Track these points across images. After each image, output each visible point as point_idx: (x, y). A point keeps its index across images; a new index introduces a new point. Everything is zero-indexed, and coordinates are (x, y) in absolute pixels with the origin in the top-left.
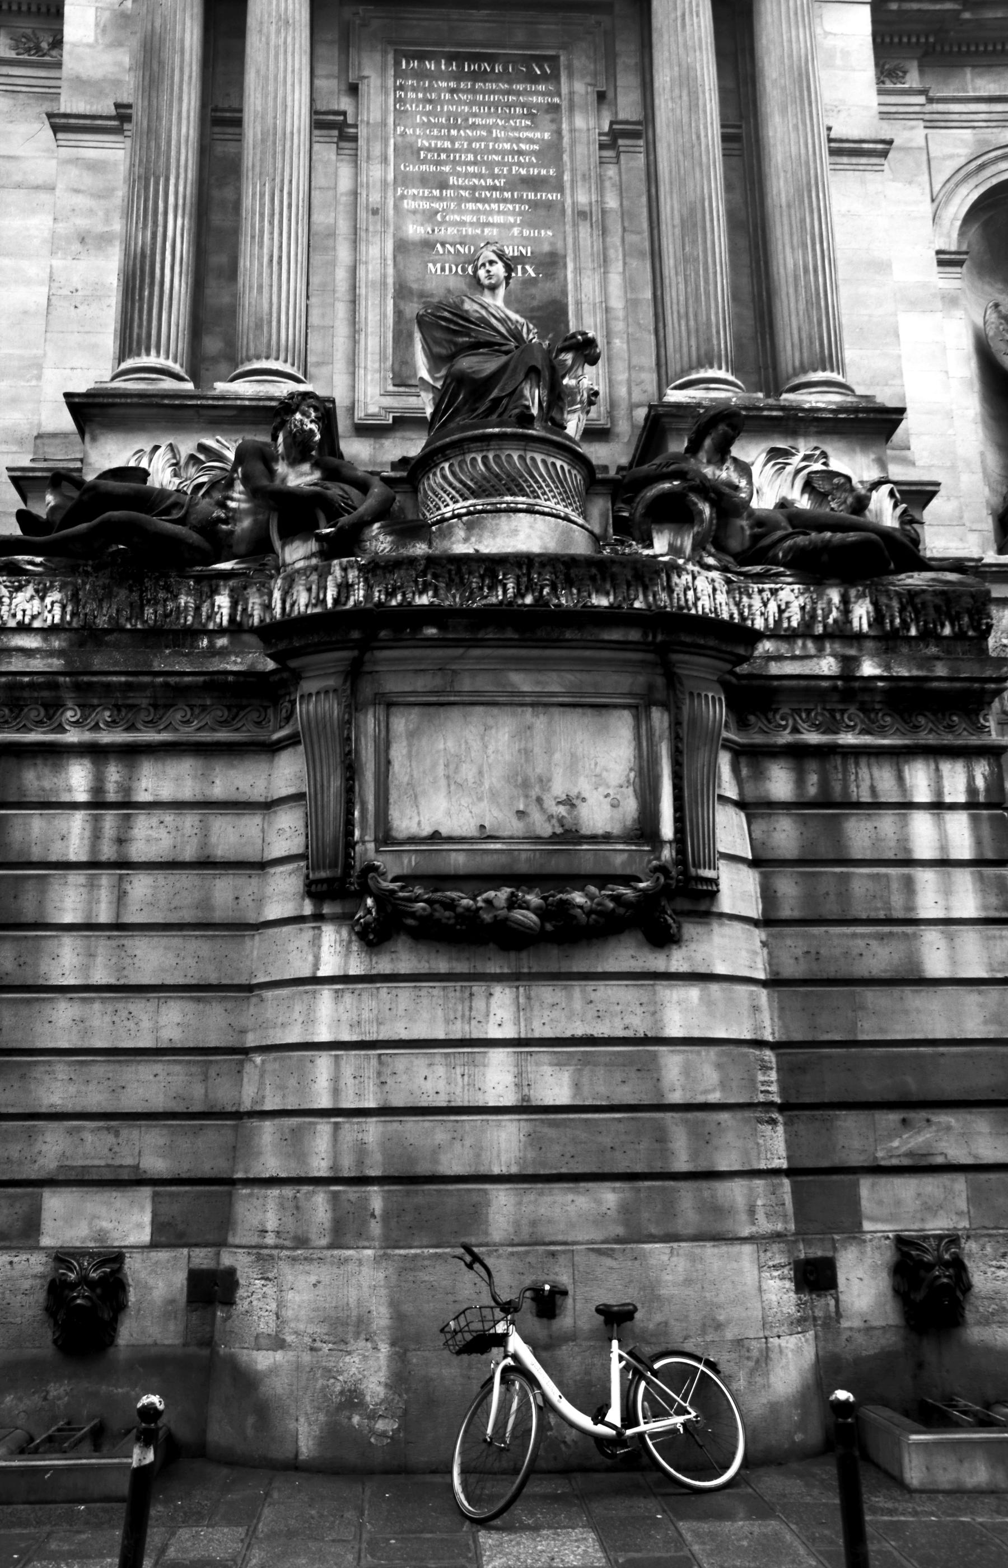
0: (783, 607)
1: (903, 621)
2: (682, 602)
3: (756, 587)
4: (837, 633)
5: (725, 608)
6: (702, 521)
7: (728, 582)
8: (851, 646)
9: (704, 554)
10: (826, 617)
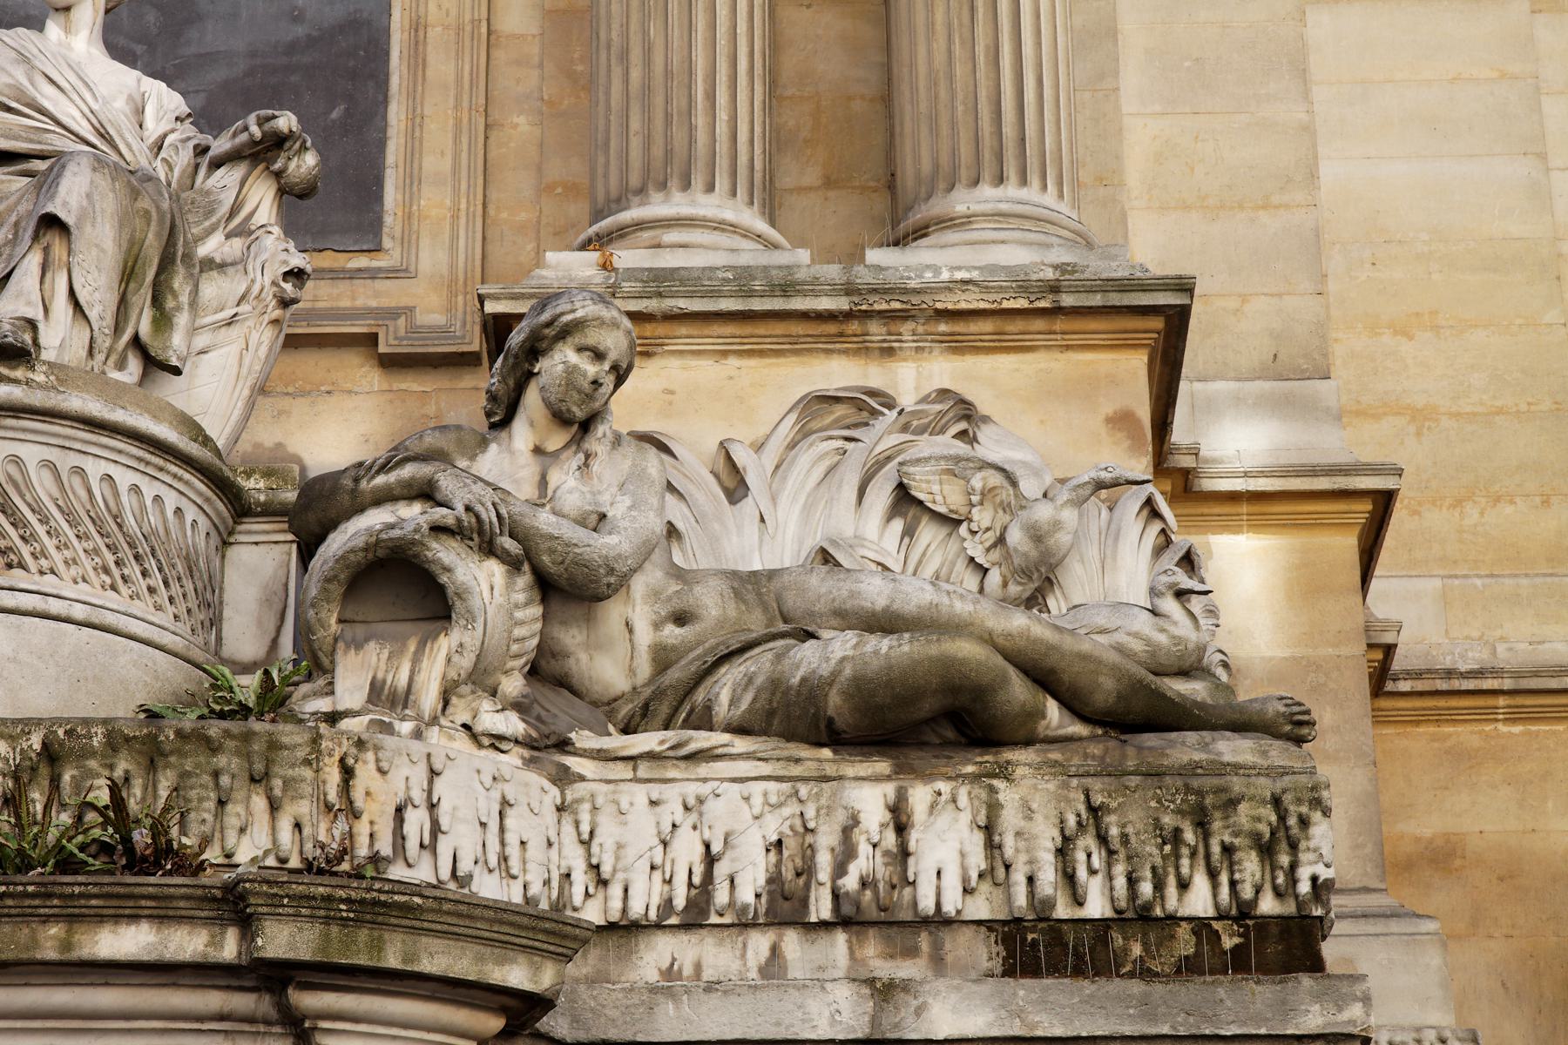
0: (716, 848)
1: (1069, 878)
2: (385, 847)
3: (640, 794)
4: (874, 914)
5: (535, 851)
6: (471, 618)
7: (563, 778)
8: (911, 952)
9: (486, 705)
10: (840, 870)
